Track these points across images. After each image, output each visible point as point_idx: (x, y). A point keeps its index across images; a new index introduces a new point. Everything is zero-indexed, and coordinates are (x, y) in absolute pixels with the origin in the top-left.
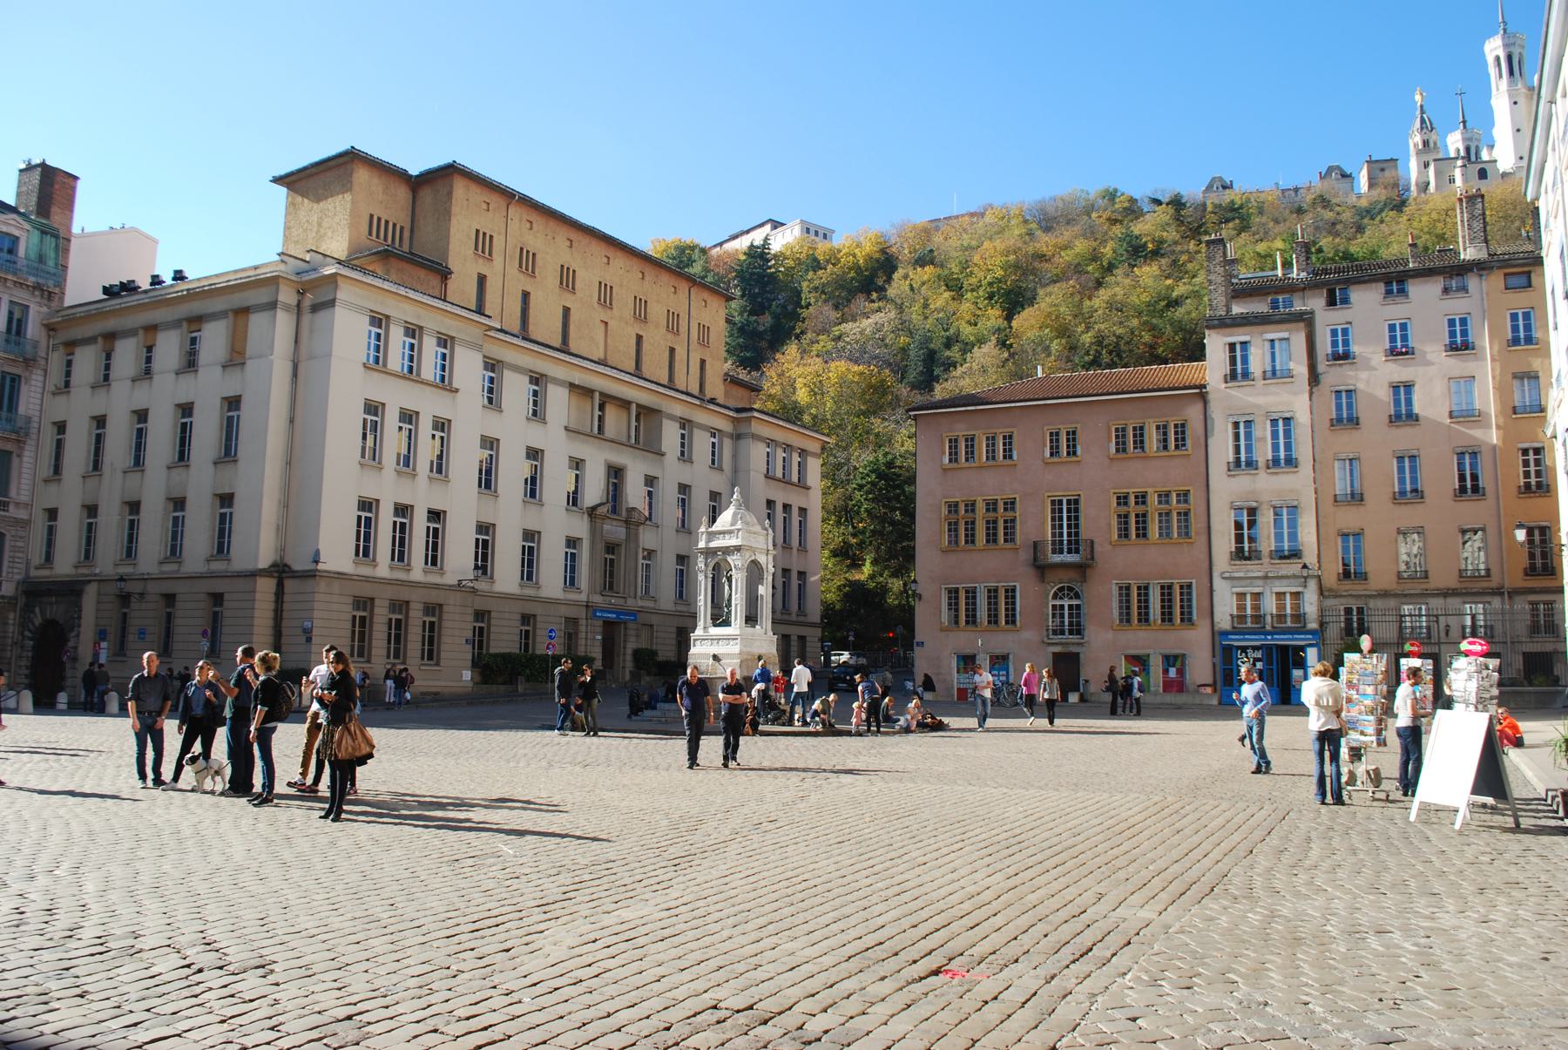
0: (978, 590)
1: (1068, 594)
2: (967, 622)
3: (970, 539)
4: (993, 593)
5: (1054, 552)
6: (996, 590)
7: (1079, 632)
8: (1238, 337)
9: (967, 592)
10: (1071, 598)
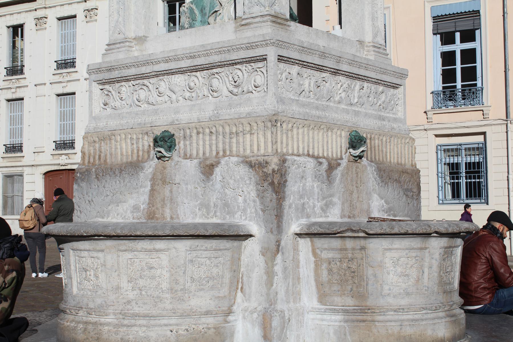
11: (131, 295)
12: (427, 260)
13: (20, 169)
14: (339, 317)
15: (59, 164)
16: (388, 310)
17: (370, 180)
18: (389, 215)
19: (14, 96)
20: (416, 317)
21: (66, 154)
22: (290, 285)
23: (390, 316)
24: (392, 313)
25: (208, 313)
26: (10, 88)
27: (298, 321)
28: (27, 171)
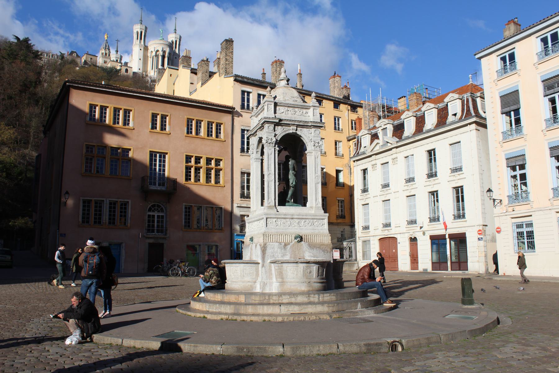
0: (105, 202)
1: (157, 209)
2: (95, 222)
4: (112, 205)
5: (151, 184)
6: (115, 203)
7: (162, 232)
8: (247, 88)
9: (96, 203)
10: (159, 211)
11: (233, 277)
12: (299, 269)
13: (369, 237)
14: (279, 284)
15: (384, 235)
19: (365, 203)
21: (387, 230)
23: (289, 284)
25: (248, 282)
26: (363, 199)
28: (372, 238)
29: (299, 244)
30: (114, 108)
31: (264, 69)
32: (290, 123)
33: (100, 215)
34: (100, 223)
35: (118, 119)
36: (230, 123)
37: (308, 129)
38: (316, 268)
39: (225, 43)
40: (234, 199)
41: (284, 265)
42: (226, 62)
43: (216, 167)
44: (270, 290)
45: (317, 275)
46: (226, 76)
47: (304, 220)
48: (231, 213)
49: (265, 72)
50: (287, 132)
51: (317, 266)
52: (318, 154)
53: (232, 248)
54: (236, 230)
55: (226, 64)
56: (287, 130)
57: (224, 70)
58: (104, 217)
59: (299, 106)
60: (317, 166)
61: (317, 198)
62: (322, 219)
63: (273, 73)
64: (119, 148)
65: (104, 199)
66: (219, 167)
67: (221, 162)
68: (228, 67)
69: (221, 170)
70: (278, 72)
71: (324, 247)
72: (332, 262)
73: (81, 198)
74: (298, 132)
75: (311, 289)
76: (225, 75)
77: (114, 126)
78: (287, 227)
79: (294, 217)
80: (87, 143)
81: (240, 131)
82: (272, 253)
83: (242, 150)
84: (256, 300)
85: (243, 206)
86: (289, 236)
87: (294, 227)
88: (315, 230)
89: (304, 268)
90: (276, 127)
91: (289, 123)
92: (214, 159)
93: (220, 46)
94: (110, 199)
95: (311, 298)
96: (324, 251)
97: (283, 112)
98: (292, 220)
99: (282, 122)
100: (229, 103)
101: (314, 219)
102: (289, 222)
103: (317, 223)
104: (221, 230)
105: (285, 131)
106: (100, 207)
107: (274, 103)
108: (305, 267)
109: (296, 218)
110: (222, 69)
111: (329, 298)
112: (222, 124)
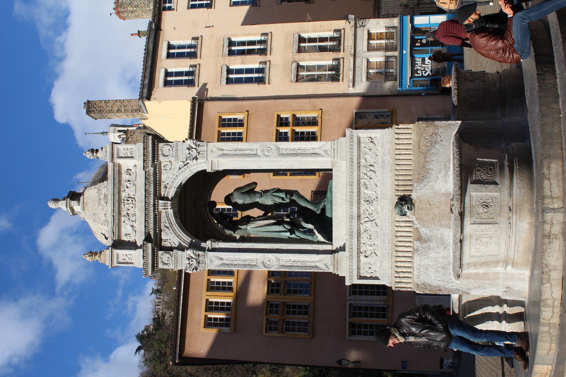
0: (352, 302)
2: (384, 316)
3: (303, 310)
9: (354, 315)
12: (477, 233)
16: (508, 255)
17: (426, 192)
18: (449, 168)
20: (513, 239)
22: (489, 282)
24: (509, 253)
27: (510, 279)
29: (416, 205)
30: (207, 291)
31: (132, 35)
32: (152, 214)
33: (372, 308)
34: (384, 309)
35: (224, 283)
36: (219, 103)
37: (163, 171)
38: (476, 190)
39: (92, 115)
40: (341, 92)
41: (466, 260)
42: (123, 111)
43: (291, 125)
44: (523, 280)
45: (492, 186)
46: (145, 111)
47: (363, 189)
48: (365, 97)
49: (137, 32)
50: (173, 219)
51: (471, 188)
52: (215, 150)
53: (423, 94)
54: (393, 86)
55: (126, 111)
56: (169, 220)
57: (135, 114)
58: (376, 303)
59: (116, 191)
60: (242, 152)
61: (312, 151)
62: (359, 142)
63: (137, 17)
64: (269, 282)
65: (348, 303)
66: (290, 120)
67: (282, 116)
68: (129, 108)
69: (294, 116)
70: (135, 9)
71: (423, 142)
72: (460, 122)
73: (347, 338)
74: (171, 193)
75: (527, 206)
76: (143, 112)
77: (235, 290)
78: (378, 229)
79: (355, 215)
80: (264, 330)
81: (230, 86)
82: (437, 270)
83: (261, 81)
84: (548, 348)
85: (351, 77)
86: (400, 229)
87: (377, 213)
88: (384, 161)
89: (474, 223)
90: (164, 244)
91: (152, 217)
92: (278, 128)
93: (99, 120)
94: (348, 294)
95: (553, 232)
96: (433, 144)
97: (132, 226)
98: (362, 217)
99: (152, 233)
100: (186, 107)
101: (359, 163)
102: (368, 225)
103: (367, 157)
104: (392, 112)
105: (170, 223)
106: (360, 308)
107: (117, 248)
108: (474, 219)
109: (359, 208)
110: (134, 116)
111: (554, 182)
112: (220, 117)
